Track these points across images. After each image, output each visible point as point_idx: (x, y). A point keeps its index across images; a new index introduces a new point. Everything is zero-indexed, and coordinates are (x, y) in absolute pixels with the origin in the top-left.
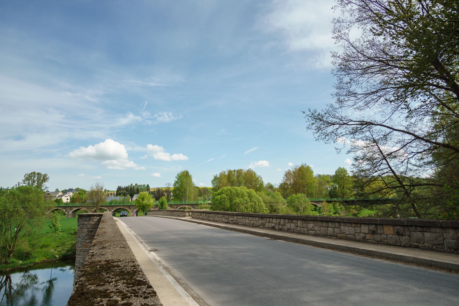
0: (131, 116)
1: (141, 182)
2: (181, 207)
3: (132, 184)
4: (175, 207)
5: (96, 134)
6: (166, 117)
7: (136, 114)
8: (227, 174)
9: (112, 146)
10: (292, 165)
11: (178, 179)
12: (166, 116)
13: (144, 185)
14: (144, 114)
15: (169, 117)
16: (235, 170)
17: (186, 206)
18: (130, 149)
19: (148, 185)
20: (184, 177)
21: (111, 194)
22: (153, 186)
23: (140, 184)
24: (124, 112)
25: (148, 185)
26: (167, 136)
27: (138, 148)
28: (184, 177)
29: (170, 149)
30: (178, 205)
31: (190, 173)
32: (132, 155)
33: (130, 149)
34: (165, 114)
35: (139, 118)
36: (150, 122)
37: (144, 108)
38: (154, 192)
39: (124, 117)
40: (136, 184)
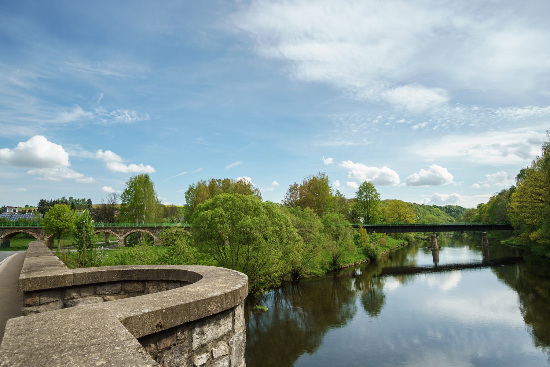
0: (79, 112)
1: (78, 196)
2: (133, 231)
3: (63, 198)
4: (123, 231)
5: (22, 131)
6: (127, 116)
7: (86, 108)
8: (207, 184)
9: (42, 147)
10: (300, 179)
11: (130, 187)
12: (127, 115)
13: (84, 200)
14: (97, 110)
15: (131, 116)
16: (219, 181)
17: (142, 231)
18: (73, 153)
19: (89, 200)
20: (140, 187)
21: (30, 211)
22: (96, 202)
23: (77, 198)
24: (69, 105)
25: (89, 200)
26: (126, 141)
27: (85, 154)
28: (140, 187)
29: (128, 156)
30: (127, 228)
31: (151, 179)
32: (75, 163)
33: (73, 153)
34: (126, 112)
35: (90, 115)
36: (105, 121)
37: (98, 102)
38: (98, 209)
39: (69, 112)
40: (70, 198)
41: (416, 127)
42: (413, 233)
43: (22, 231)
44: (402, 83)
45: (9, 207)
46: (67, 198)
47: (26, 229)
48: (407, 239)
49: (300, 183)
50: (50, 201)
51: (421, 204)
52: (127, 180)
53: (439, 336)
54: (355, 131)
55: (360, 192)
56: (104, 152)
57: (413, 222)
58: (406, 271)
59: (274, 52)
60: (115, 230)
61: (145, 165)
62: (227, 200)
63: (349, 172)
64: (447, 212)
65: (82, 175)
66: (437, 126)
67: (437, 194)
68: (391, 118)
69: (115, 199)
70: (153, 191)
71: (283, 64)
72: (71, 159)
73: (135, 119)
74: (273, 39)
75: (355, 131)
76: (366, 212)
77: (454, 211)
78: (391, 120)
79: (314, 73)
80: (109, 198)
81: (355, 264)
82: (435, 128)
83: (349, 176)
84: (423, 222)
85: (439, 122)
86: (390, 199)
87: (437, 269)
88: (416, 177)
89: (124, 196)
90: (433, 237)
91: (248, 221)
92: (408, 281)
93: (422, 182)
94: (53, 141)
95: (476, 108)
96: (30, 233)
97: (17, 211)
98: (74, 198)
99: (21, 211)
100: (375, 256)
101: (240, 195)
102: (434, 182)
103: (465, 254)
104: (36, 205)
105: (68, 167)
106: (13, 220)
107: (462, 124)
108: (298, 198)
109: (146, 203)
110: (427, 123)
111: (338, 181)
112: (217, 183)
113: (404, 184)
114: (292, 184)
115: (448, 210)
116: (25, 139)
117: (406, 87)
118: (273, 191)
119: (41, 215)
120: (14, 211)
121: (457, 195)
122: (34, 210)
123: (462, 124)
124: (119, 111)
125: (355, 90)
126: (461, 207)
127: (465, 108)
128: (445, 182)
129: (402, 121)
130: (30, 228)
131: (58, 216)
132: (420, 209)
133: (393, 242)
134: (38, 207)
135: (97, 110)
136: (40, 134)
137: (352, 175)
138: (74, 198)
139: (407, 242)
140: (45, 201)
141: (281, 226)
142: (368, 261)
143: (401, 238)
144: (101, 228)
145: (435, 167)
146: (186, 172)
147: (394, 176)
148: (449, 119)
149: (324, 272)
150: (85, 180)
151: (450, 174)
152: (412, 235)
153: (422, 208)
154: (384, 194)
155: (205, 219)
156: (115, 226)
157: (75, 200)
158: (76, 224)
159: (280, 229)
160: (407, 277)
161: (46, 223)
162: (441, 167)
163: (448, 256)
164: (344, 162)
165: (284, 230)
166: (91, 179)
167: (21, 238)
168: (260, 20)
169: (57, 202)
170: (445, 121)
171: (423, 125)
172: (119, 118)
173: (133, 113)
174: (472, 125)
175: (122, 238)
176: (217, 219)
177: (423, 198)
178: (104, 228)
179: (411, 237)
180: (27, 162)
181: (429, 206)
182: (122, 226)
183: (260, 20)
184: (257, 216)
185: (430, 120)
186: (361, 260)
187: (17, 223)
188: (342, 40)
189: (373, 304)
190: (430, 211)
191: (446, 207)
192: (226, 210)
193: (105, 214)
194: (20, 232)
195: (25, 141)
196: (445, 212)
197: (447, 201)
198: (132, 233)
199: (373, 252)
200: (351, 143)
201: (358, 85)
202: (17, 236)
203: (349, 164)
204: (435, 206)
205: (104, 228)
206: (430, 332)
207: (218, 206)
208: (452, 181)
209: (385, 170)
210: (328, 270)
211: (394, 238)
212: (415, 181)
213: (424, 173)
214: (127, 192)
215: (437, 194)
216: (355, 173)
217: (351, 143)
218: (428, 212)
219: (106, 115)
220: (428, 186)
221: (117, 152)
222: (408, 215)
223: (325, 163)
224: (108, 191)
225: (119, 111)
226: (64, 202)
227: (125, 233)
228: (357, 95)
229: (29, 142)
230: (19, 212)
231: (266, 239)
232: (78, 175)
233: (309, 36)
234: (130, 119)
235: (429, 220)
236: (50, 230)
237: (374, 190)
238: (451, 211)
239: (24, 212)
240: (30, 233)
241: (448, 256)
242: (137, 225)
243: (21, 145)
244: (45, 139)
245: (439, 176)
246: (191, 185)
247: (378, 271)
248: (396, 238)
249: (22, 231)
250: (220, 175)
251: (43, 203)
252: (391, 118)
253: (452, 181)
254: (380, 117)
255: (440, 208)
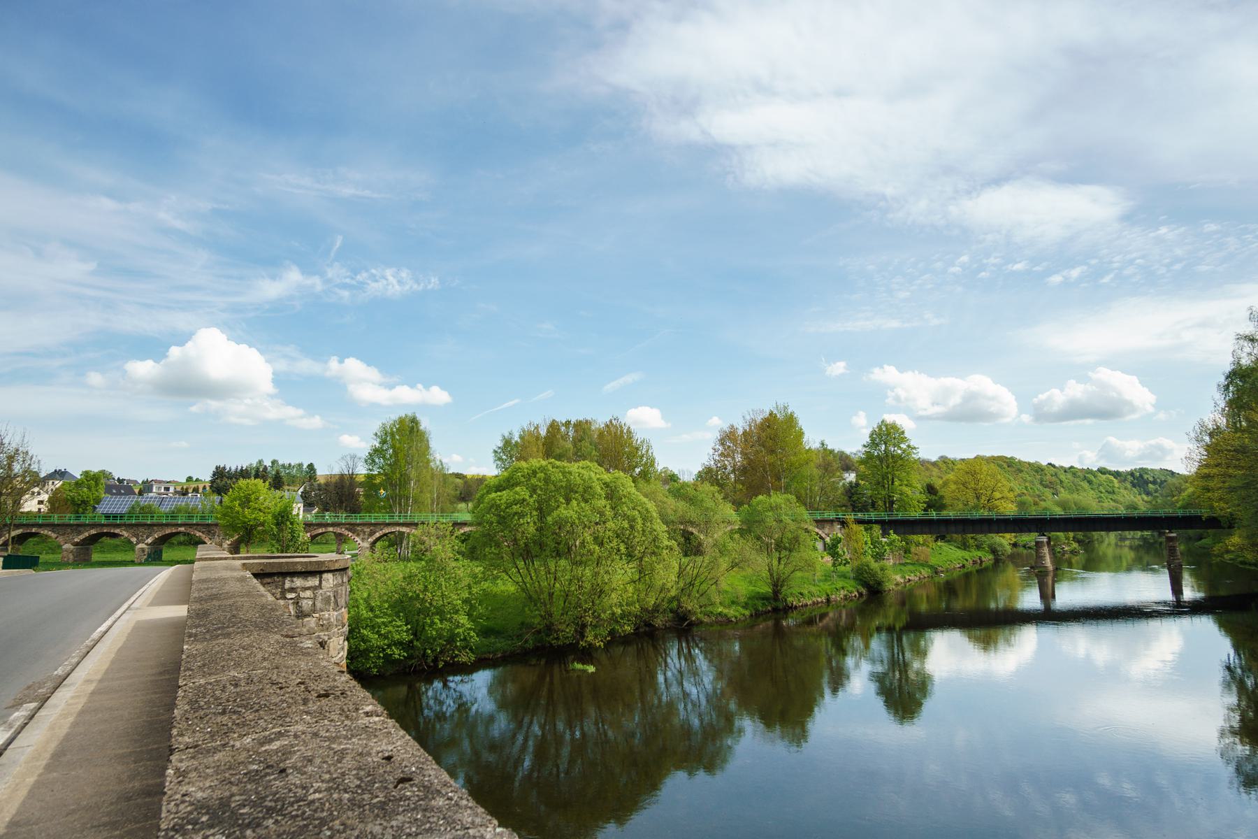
0: (294, 276)
1: (290, 456)
2: (386, 530)
3: (260, 462)
4: (367, 530)
5: (180, 320)
6: (392, 282)
7: (308, 268)
8: (543, 432)
9: (218, 353)
10: (741, 413)
11: (383, 442)
12: (391, 278)
13: (300, 465)
14: (330, 273)
15: (400, 282)
16: (568, 423)
17: (404, 529)
18: (282, 366)
19: (311, 466)
20: (404, 439)
21: (196, 490)
22: (328, 468)
23: (287, 463)
24: (272, 264)
25: (311, 466)
26: (389, 335)
27: (306, 366)
28: (404, 439)
30: (375, 525)
31: (424, 424)
32: (285, 385)
33: (282, 366)
34: (389, 273)
35: (316, 283)
36: (346, 294)
37: (332, 254)
38: (327, 484)
39: (273, 277)
40: (274, 462)
41: (1057, 279)
42: (1008, 535)
43: (182, 529)
44: (998, 180)
45: (156, 481)
46: (268, 463)
47: (191, 525)
48: (993, 551)
49: (741, 426)
50: (233, 469)
51: (1067, 465)
52: (376, 426)
53: (1128, 789)
54: (903, 295)
55: (874, 443)
56: (341, 362)
57: (1009, 509)
58: (989, 623)
59: (689, 130)
60: (352, 527)
61: (427, 387)
62: (535, 473)
63: (890, 393)
64: (1134, 485)
65: (301, 412)
66: (1112, 276)
67: (1112, 439)
68: (992, 260)
69: (355, 466)
70: (428, 447)
71: (711, 156)
72: (278, 380)
73: (407, 287)
74: (685, 102)
75: (903, 295)
76: (882, 492)
77: (1154, 483)
78: (993, 265)
79: (786, 169)
80: (343, 464)
81: (828, 600)
82: (1106, 280)
83: (890, 401)
84: (1045, 509)
85: (1116, 265)
86: (988, 454)
87: (1049, 616)
88: (1058, 397)
89: (371, 460)
90: (1038, 544)
91: (567, 512)
92: (1001, 644)
93: (1074, 412)
94: (239, 341)
95: (1212, 227)
96: (198, 534)
97: (172, 490)
98: (280, 462)
99: (179, 489)
100: (880, 583)
101: (558, 463)
102: (1106, 411)
103: (1150, 587)
104: (206, 476)
105: (272, 396)
106: (165, 509)
107: (1177, 267)
108: (738, 458)
109: (413, 474)
110: (1085, 268)
111: (862, 413)
112: (563, 429)
113: (1026, 418)
114: (726, 427)
115: (1139, 479)
116: (182, 338)
117: (1007, 188)
118: (683, 444)
119: (216, 498)
120: (167, 489)
121: (1167, 443)
122: (204, 488)
123: (1177, 267)
124: (373, 271)
125: (882, 204)
126: (1173, 473)
127: (1183, 229)
128: (1133, 409)
129: (1018, 267)
130: (197, 525)
131: (246, 502)
132: (1063, 477)
133: (949, 556)
134: (212, 482)
135: (330, 273)
136: (217, 325)
137: (897, 399)
138: (280, 462)
139: (991, 557)
140: (224, 468)
141: (634, 520)
142: (861, 595)
143: (978, 547)
144: (327, 525)
145: (1104, 374)
146: (517, 401)
147: (1003, 398)
148: (1143, 257)
149: (747, 613)
150: (305, 420)
151: (1146, 389)
152: (1005, 540)
153: (1069, 476)
154: (927, 446)
155: (494, 506)
156: (353, 521)
157: (283, 466)
158: (274, 517)
159: (632, 527)
160: (1002, 634)
161: (225, 515)
162: (1118, 373)
163: (1101, 589)
164: (876, 370)
165: (639, 527)
166: (317, 422)
167: (180, 544)
168: (657, 58)
169: (244, 474)
170: (1131, 262)
171: (1075, 273)
172: (375, 288)
173: (404, 274)
174: (1203, 268)
175: (366, 545)
176: (516, 508)
177: (1076, 451)
178: (333, 525)
179: (1001, 545)
180: (186, 388)
181: (1089, 471)
182: (367, 520)
183: (657, 58)
184: (586, 502)
185: (1093, 262)
186: (843, 593)
187: (173, 514)
188: (840, 93)
189: (903, 696)
190: (1090, 482)
191: (1132, 474)
192: (533, 490)
193: (340, 495)
194: (178, 533)
195: (181, 343)
196: (1129, 486)
197: (1141, 457)
198: (385, 535)
199: (874, 575)
200: (895, 324)
201: (889, 191)
202: (174, 540)
203: (888, 374)
204: (1102, 471)
205: (333, 525)
206: (1104, 780)
207: (517, 484)
208: (1151, 409)
209: (982, 383)
210: (757, 610)
211: (975, 548)
212: (1055, 408)
213: (1075, 391)
214: (377, 452)
215: (1112, 439)
216: (903, 394)
217: (895, 324)
218: (1085, 485)
219: (348, 280)
220: (1089, 421)
221: (368, 361)
222: (997, 495)
223: (828, 373)
224: (344, 450)
225: (373, 271)
226: (259, 473)
227: (371, 534)
228: (890, 216)
229: (190, 344)
230: (176, 492)
231: (601, 544)
232: (291, 411)
233: (763, 89)
234: (397, 287)
235: (1063, 505)
236: (233, 527)
237: (904, 440)
238: (1147, 482)
239: (184, 493)
240: (198, 534)
241: (1101, 589)
242: (396, 519)
243: (175, 352)
244: (224, 337)
245: (1115, 395)
246: (506, 435)
247: (886, 617)
248: (965, 546)
249: (182, 529)
250: (569, 411)
251: (220, 473)
252: (992, 260)
253: (1151, 409)
254: (965, 258)
255: (1117, 474)
